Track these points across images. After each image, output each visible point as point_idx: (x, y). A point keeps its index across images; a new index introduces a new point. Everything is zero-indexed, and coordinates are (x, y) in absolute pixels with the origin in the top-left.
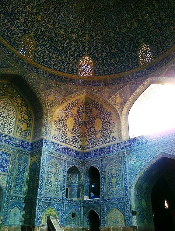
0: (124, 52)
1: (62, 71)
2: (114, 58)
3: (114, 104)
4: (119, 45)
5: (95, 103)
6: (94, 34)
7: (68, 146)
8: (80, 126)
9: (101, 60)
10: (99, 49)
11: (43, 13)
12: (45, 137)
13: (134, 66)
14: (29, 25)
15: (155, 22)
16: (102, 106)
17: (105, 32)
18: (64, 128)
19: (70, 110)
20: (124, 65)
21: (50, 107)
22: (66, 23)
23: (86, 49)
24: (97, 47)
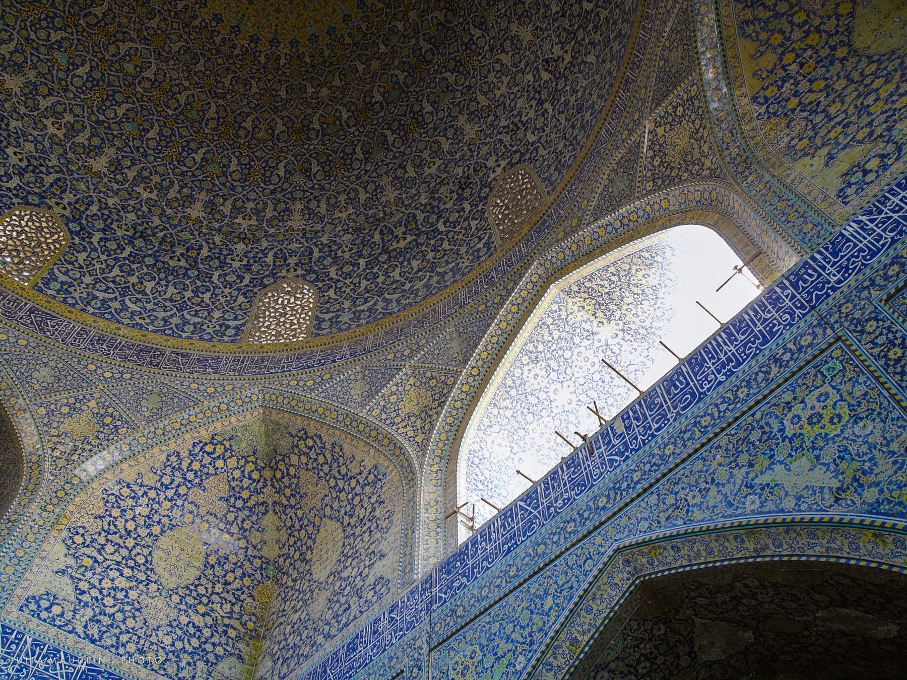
2: (402, 263)
3: (393, 424)
4: (420, 217)
5: (310, 443)
6: (323, 208)
8: (247, 581)
9: (351, 283)
14: (49, 179)
15: (534, 87)
16: (337, 449)
17: (367, 192)
18: (127, 572)
19: (182, 490)
20: (439, 274)
22: (214, 185)
23: (292, 261)
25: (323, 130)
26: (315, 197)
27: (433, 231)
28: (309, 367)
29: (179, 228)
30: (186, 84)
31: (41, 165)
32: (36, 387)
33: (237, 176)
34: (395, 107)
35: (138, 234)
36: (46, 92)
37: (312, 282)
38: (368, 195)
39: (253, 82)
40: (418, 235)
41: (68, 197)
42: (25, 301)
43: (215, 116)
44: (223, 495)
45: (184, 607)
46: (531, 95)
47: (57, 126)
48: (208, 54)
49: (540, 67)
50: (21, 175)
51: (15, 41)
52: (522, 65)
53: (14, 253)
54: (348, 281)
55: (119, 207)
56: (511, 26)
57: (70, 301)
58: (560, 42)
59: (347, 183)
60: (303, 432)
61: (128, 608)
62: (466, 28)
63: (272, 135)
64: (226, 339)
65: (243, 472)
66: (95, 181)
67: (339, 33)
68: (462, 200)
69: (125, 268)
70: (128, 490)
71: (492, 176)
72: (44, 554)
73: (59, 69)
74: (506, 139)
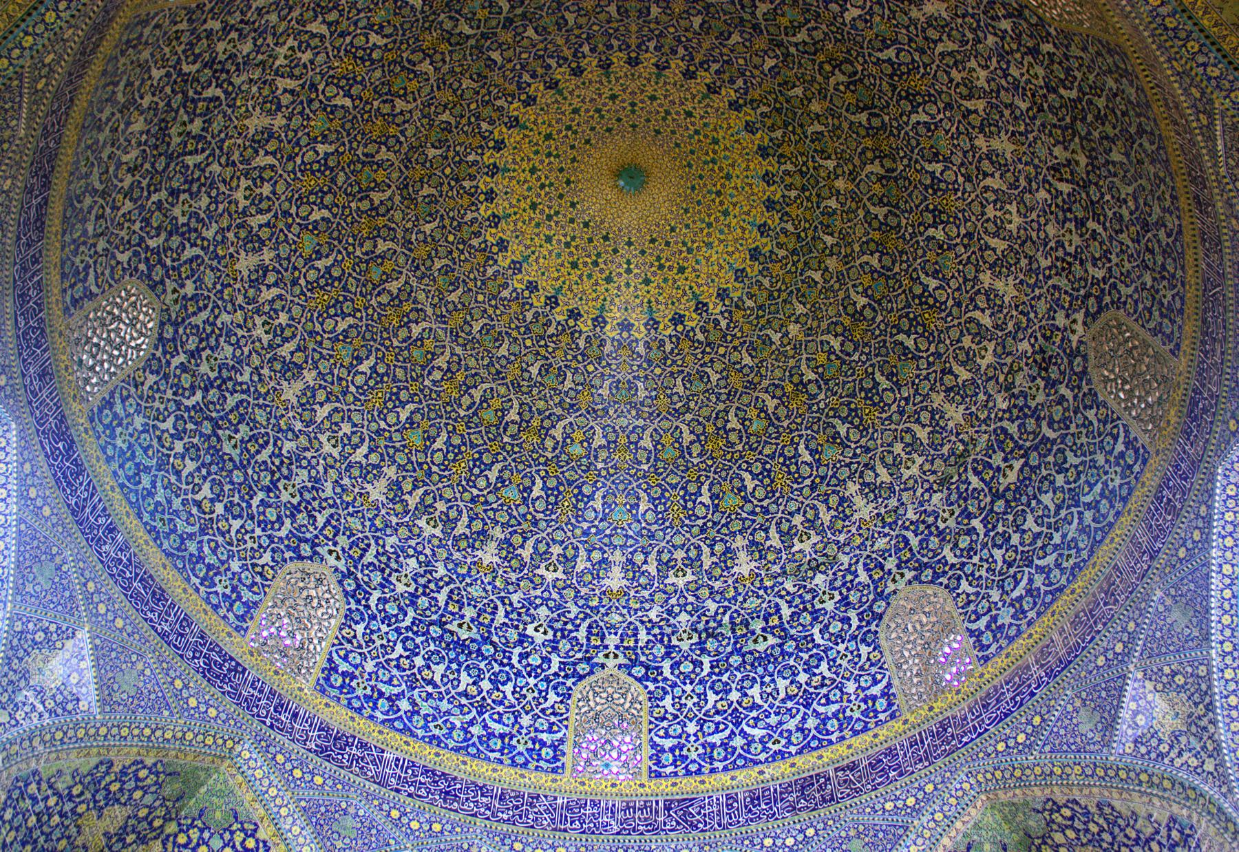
0: (1054, 442)
1: (814, 744)
2: (1029, 505)
4: (1013, 429)
5: (1068, 813)
6: (884, 476)
9: (981, 560)
10: (945, 521)
13: (1130, 467)
14: (581, 634)
16: (1107, 810)
17: (924, 426)
20: (1088, 506)
22: (743, 520)
23: (890, 564)
24: (931, 520)
25: (821, 375)
26: (866, 465)
27: (1041, 442)
28: (1006, 715)
29: (740, 599)
30: (641, 422)
31: (565, 623)
33: (760, 493)
35: (704, 635)
37: (932, 582)
38: (928, 429)
41: (612, 640)
43: (693, 437)
52: (1023, 183)
53: (608, 747)
54: (976, 559)
56: (977, 143)
57: (693, 768)
59: (893, 427)
63: (767, 416)
64: (882, 716)
68: (1053, 386)
69: (719, 686)
71: (1074, 338)
74: (1063, 282)
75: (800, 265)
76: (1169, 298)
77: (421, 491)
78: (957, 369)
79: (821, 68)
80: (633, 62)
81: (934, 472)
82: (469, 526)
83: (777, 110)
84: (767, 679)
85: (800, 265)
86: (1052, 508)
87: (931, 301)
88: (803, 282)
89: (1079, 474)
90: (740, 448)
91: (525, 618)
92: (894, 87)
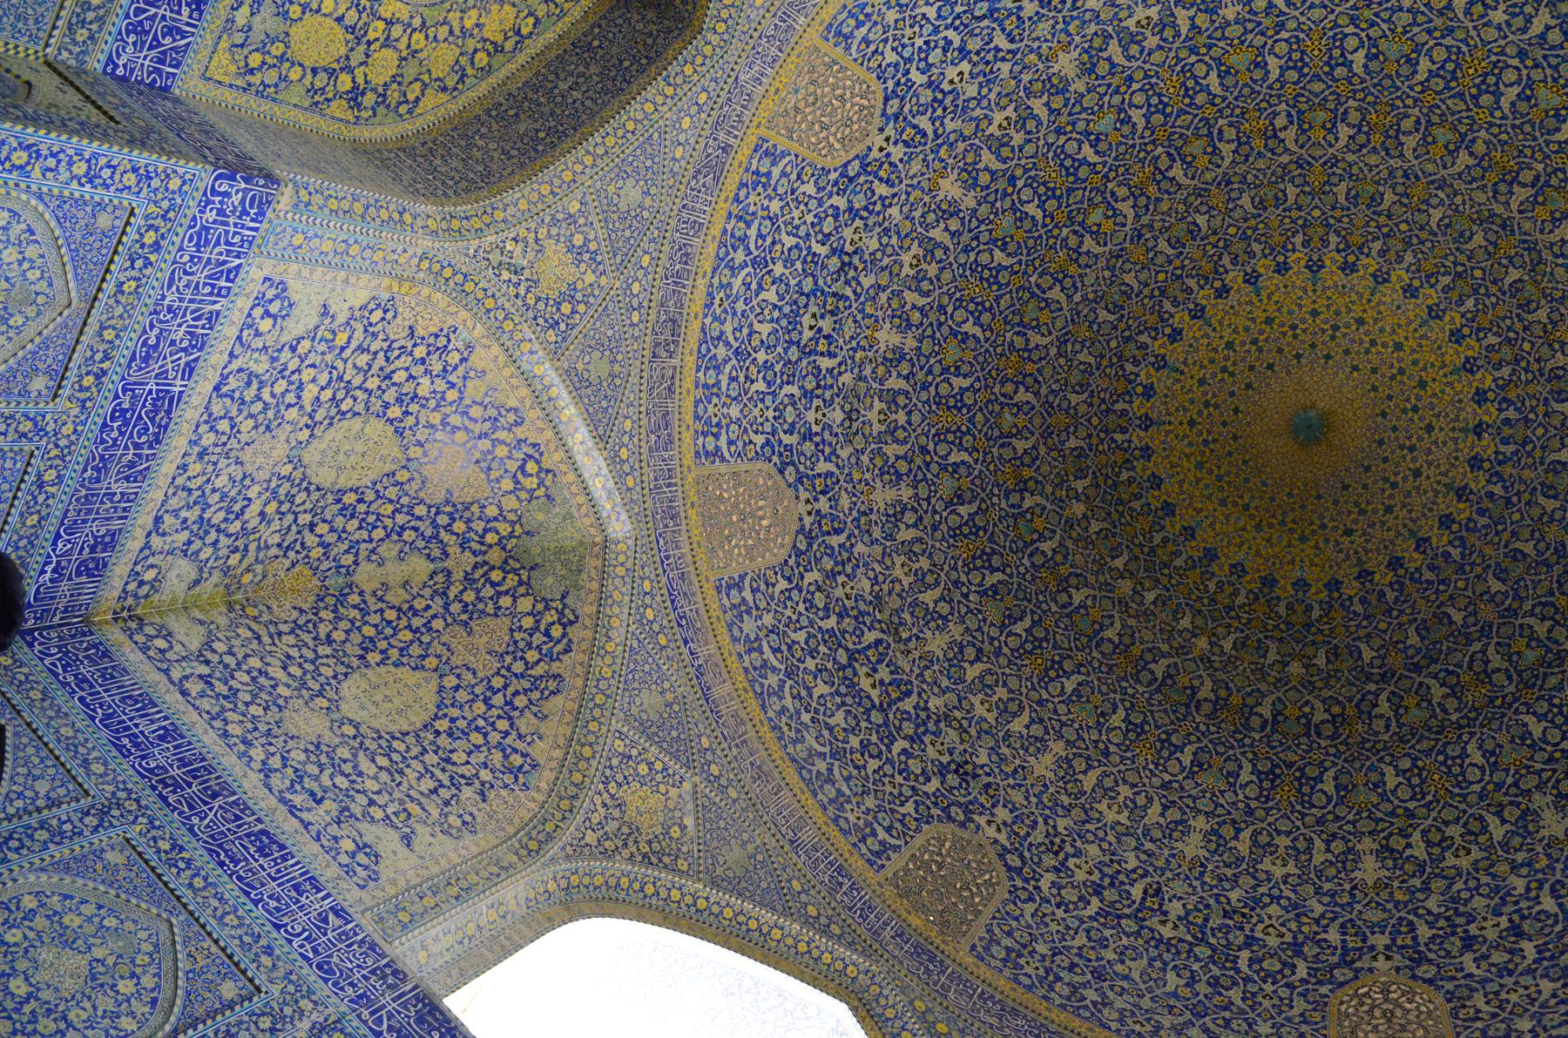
2: (838, 693)
4: (908, 705)
6: (905, 535)
7: (177, 443)
9: (801, 614)
11: (975, 211)
12: (285, 198)
14: (924, 122)
15: (1119, 872)
16: (552, 685)
17: (936, 602)
18: (328, 394)
20: (830, 770)
21: (495, 257)
22: (927, 358)
23: (823, 504)
24: (849, 570)
25: (1022, 514)
26: (921, 519)
27: (891, 733)
28: (673, 602)
29: (859, 317)
30: (1077, 298)
31: (945, 109)
32: (611, 189)
33: (944, 389)
34: (1066, 629)
35: (846, 259)
36: (1054, 106)
38: (931, 606)
39: (1085, 396)
40: (881, 709)
41: (897, 152)
42: (740, 134)
44: (456, 494)
45: (273, 485)
46: (1107, 870)
47: (1005, 124)
48: (1122, 326)
49: (1149, 880)
50: (930, 84)
51: (1127, 64)
52: (1148, 846)
53: (811, 99)
55: (886, 224)
58: (1188, 913)
59: (946, 568)
60: (572, 618)
61: (270, 414)
62: (1193, 738)
64: (700, 442)
65: (495, 519)
66: (925, 184)
67: (1167, 522)
68: (940, 773)
70: (457, 361)
71: (982, 820)
72: (353, 280)
73: (1088, 122)
74: (1038, 836)
75: (1137, 551)
76: (1028, 970)
77: (1184, 31)
78: (979, 667)
79: (1339, 703)
80: (1446, 521)
81: (890, 593)
82: (1109, 59)
83: (1308, 626)
84: (776, 314)
85: (1137, 551)
86: (831, 721)
87: (1052, 674)
88: (1120, 544)
89: (857, 767)
90: (996, 390)
91: (981, 67)
92: (1290, 765)
